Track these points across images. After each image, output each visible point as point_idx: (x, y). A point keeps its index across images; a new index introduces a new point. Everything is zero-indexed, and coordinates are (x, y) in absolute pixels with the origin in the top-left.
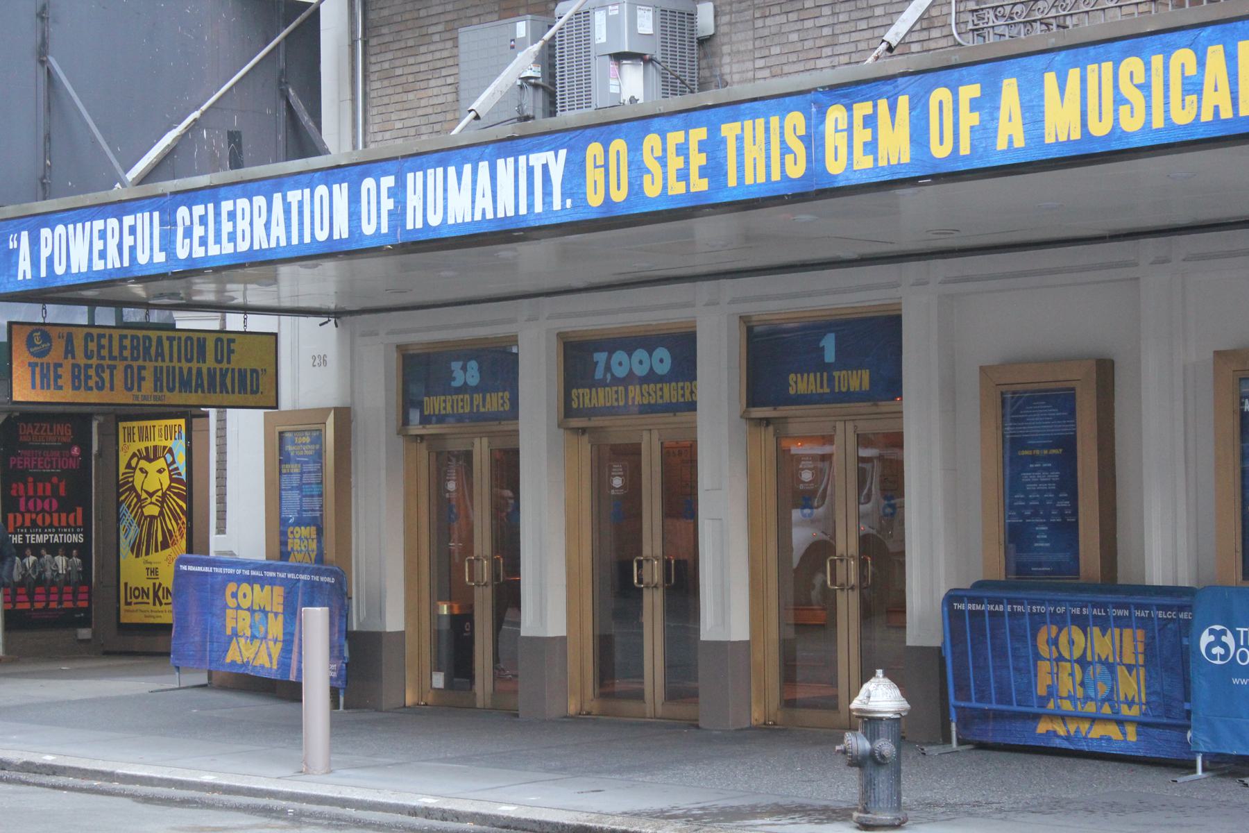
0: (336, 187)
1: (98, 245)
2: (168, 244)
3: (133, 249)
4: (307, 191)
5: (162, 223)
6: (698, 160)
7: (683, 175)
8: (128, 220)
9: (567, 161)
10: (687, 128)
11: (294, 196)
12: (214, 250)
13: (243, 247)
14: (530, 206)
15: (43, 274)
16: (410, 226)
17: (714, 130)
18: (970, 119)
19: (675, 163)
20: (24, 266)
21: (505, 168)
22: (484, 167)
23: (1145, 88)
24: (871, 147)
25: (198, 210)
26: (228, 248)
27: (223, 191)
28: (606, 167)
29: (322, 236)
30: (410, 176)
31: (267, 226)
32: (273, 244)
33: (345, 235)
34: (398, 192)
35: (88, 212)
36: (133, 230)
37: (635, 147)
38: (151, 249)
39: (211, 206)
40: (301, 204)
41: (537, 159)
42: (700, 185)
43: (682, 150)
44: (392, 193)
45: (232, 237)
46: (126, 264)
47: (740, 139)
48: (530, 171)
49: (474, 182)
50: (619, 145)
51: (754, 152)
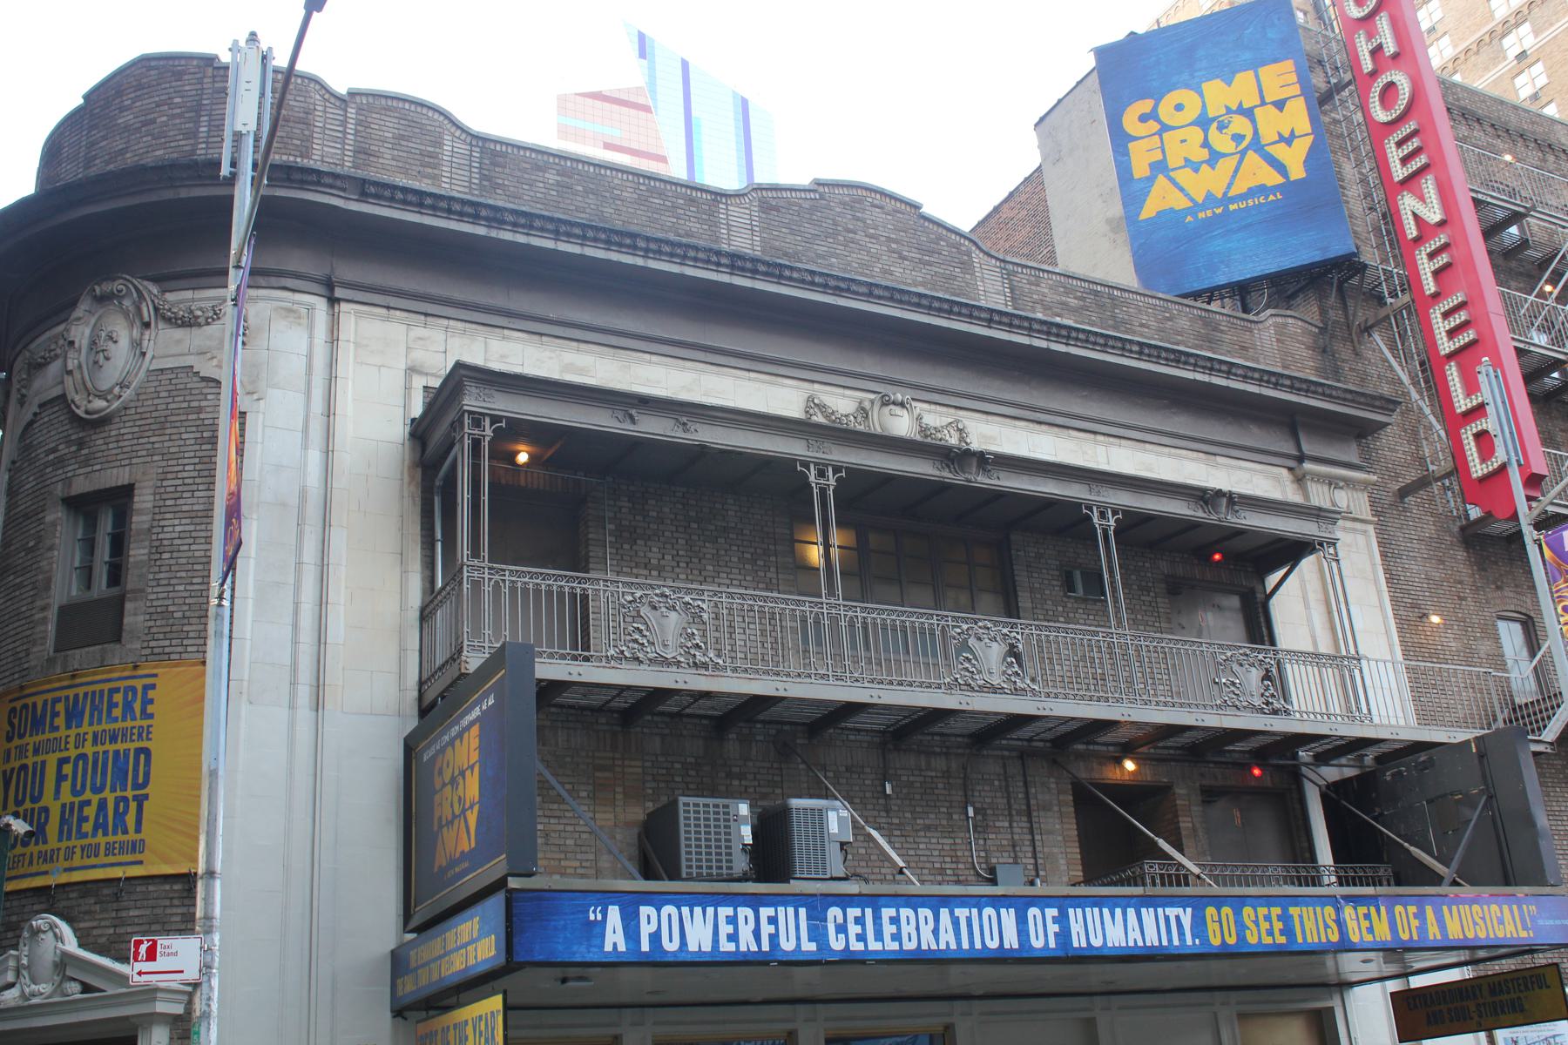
0: (1003, 911)
1: (726, 929)
2: (817, 934)
3: (774, 938)
4: (975, 911)
5: (809, 918)
6: (1278, 926)
7: (1270, 933)
8: (766, 912)
9: (1193, 916)
10: (1269, 906)
11: (961, 913)
12: (874, 946)
13: (910, 946)
14: (1170, 940)
15: (645, 946)
16: (1076, 944)
17: (1285, 910)
18: (1415, 923)
19: (1264, 926)
20: (614, 938)
21: (1148, 915)
22: (1131, 912)
23: (1483, 919)
24: (1370, 930)
25: (853, 912)
26: (895, 946)
27: (883, 900)
28: (1220, 922)
29: (993, 944)
30: (1071, 911)
31: (936, 932)
32: (943, 946)
33: (1016, 946)
34: (1062, 919)
35: (710, 898)
36: (773, 920)
37: (1238, 913)
38: (798, 938)
39: (868, 911)
40: (969, 920)
41: (1172, 912)
42: (1282, 940)
43: (1268, 918)
44: (1055, 920)
45: (897, 937)
46: (766, 947)
47: (1301, 916)
48: (1167, 919)
49: (1125, 921)
50: (1226, 910)
51: (1309, 925)
